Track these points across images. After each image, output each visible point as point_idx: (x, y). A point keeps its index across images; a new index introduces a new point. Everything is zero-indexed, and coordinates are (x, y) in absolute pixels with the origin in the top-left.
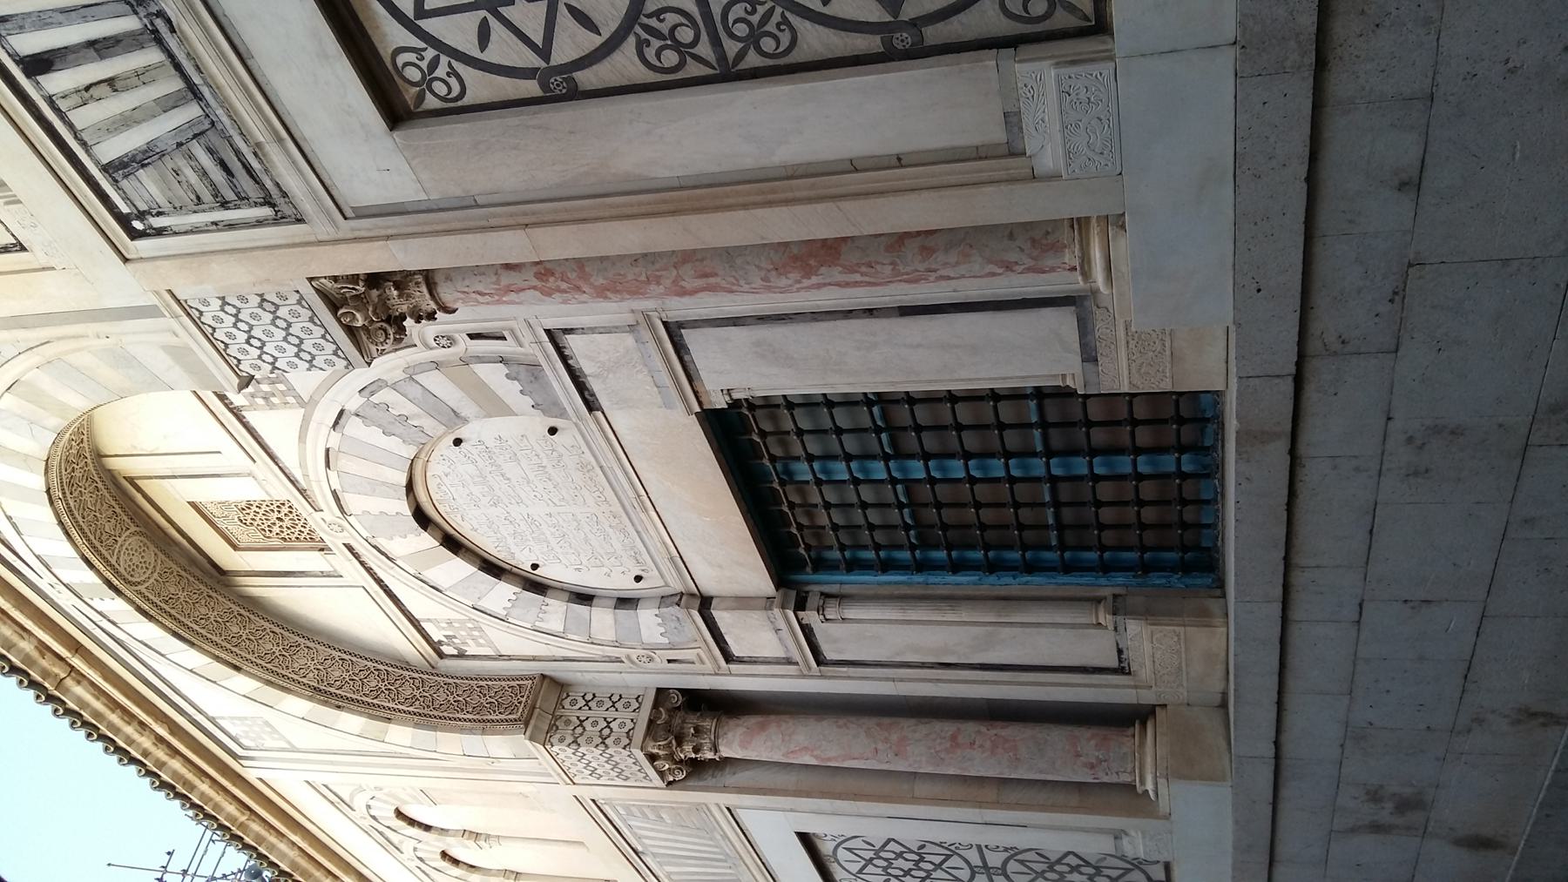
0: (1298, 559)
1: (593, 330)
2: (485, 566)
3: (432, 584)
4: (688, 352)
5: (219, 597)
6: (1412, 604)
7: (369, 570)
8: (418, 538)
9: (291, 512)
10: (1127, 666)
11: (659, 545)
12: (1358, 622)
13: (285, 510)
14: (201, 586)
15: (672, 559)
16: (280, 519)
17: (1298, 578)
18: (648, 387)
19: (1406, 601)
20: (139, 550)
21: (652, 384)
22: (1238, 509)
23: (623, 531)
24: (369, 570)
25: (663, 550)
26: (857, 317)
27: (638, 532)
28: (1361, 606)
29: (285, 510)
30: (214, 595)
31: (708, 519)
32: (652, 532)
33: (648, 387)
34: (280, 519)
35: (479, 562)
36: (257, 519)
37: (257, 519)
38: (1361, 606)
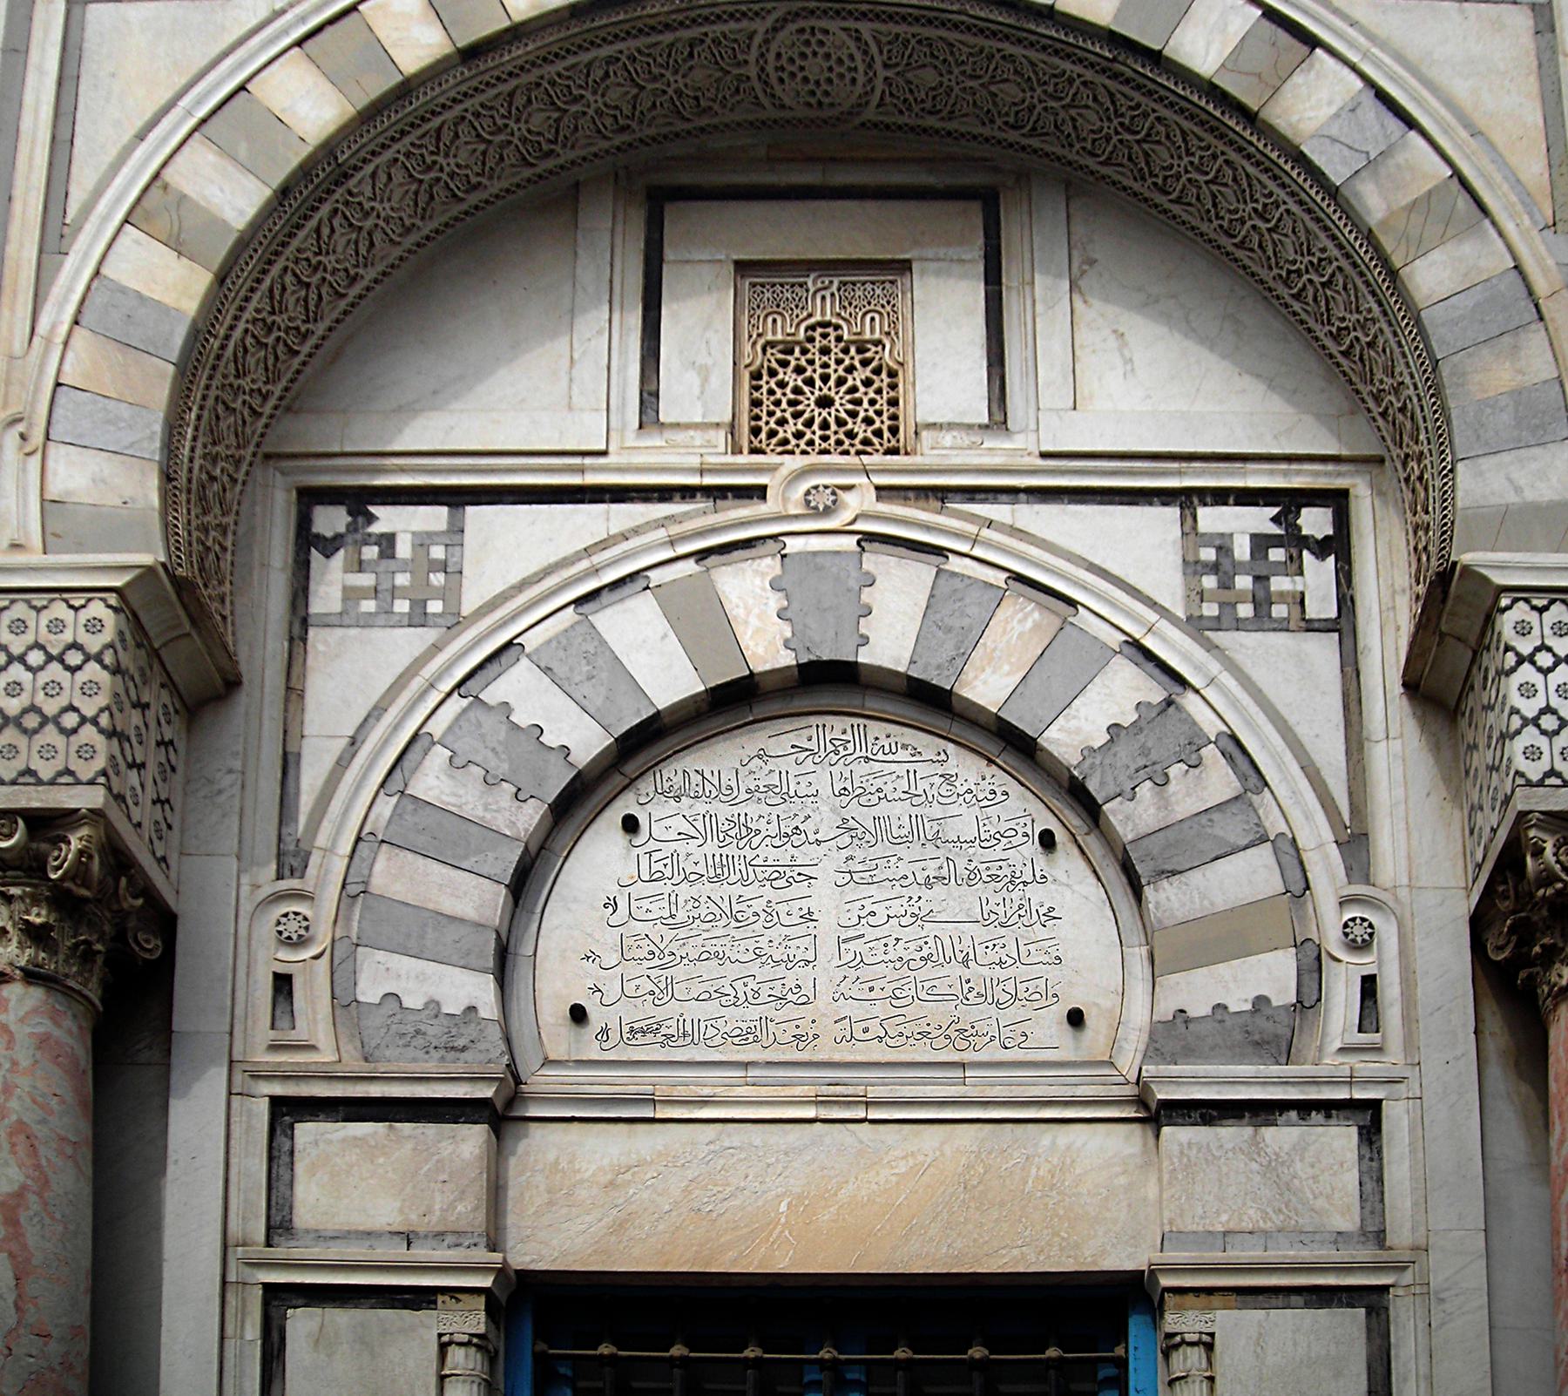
2: (655, 726)
3: (606, 597)
4: (1307, 1306)
5: (605, 144)
8: (780, 644)
11: (706, 1091)
14: (652, 131)
18: (1224, 1218)
20: (825, 87)
21: (1232, 1226)
23: (746, 1036)
30: (618, 140)
31: (783, 1207)
33: (1224, 1218)
35: (666, 720)
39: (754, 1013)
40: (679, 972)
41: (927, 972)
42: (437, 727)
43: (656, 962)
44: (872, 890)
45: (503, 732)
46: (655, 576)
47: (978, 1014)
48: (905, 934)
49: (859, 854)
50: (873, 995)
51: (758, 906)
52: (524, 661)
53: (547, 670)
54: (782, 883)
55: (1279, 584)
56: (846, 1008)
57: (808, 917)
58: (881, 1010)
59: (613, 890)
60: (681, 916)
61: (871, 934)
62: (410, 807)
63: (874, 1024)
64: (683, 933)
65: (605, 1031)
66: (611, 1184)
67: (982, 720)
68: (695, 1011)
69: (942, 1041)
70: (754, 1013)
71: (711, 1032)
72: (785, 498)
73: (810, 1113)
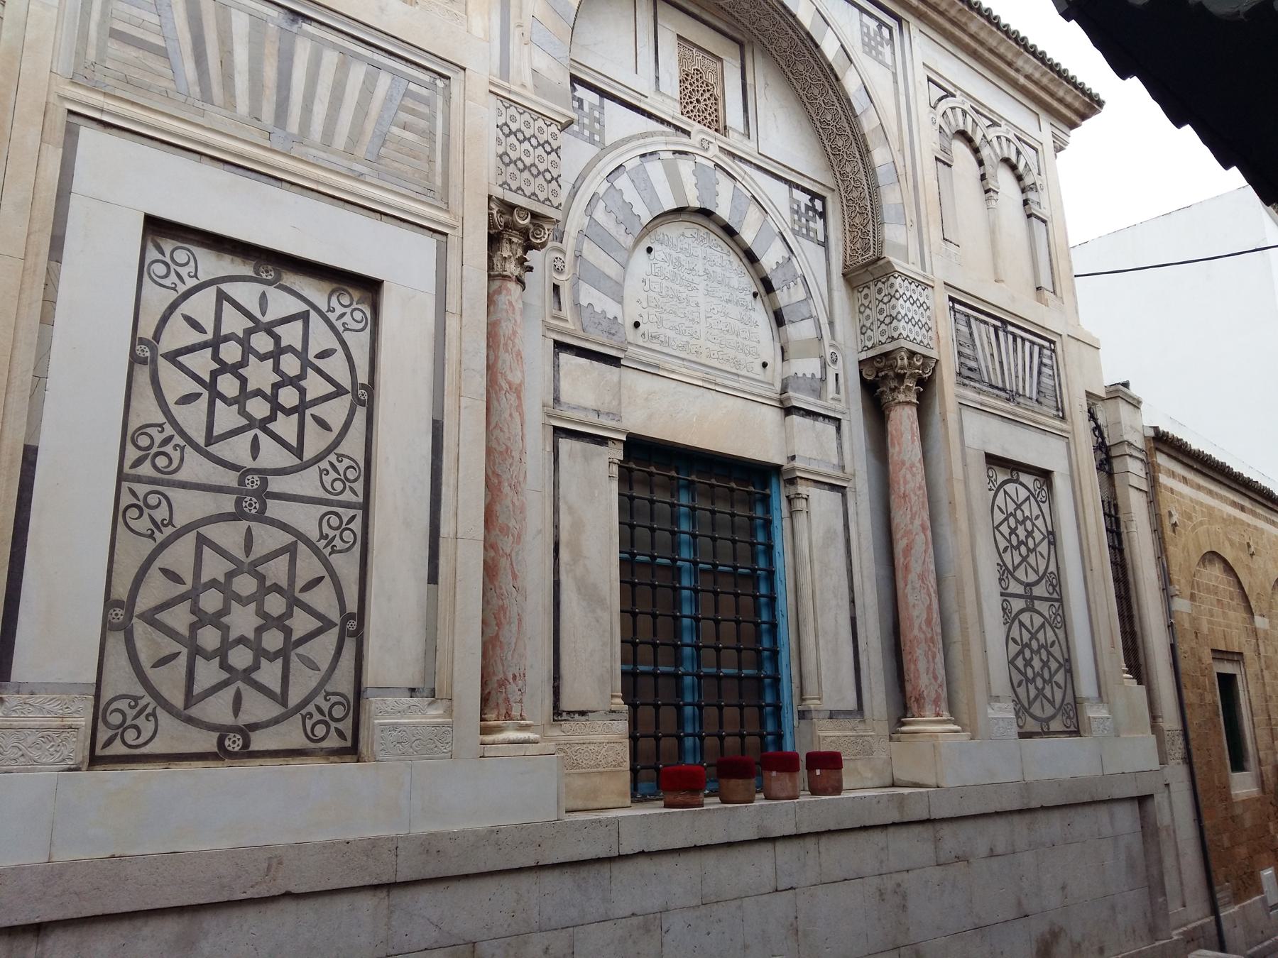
0: (824, 841)
1: (840, 446)
6: (795, 922)
7: (650, 116)
9: (687, 103)
10: (563, 718)
11: (674, 367)
12: (777, 891)
13: (690, 107)
15: (658, 367)
16: (698, 101)
17: (810, 843)
19: (796, 918)
22: (861, 798)
23: (683, 348)
24: (650, 116)
25: (667, 366)
26: (850, 594)
27: (683, 359)
28: (791, 888)
29: (690, 107)
32: (684, 370)
34: (698, 101)
36: (694, 80)
37: (694, 80)
38: (791, 888)
39: (685, 339)
40: (665, 316)
41: (728, 337)
42: (601, 192)
43: (657, 310)
44: (712, 299)
45: (620, 203)
46: (662, 155)
47: (741, 356)
48: (723, 319)
49: (710, 284)
50: (713, 341)
51: (684, 295)
52: (625, 174)
53: (633, 181)
54: (690, 289)
55: (811, 224)
56: (709, 345)
57: (697, 305)
58: (717, 347)
59: (645, 277)
60: (664, 293)
61: (714, 317)
62: (594, 224)
63: (715, 352)
64: (665, 300)
65: (644, 334)
66: (646, 399)
67: (742, 245)
68: (671, 334)
69: (732, 365)
70: (685, 339)
71: (673, 343)
72: (696, 138)
73: (700, 383)
